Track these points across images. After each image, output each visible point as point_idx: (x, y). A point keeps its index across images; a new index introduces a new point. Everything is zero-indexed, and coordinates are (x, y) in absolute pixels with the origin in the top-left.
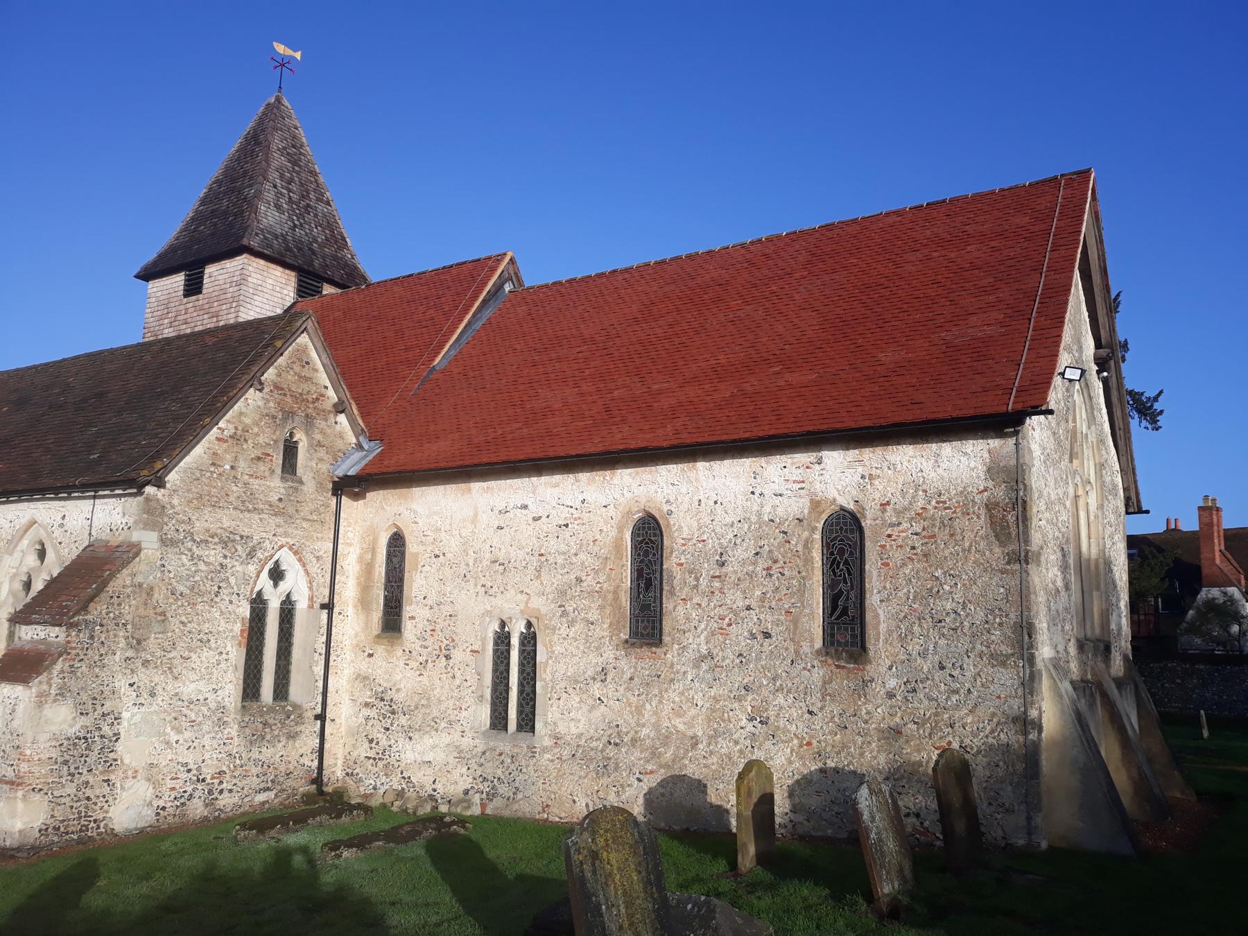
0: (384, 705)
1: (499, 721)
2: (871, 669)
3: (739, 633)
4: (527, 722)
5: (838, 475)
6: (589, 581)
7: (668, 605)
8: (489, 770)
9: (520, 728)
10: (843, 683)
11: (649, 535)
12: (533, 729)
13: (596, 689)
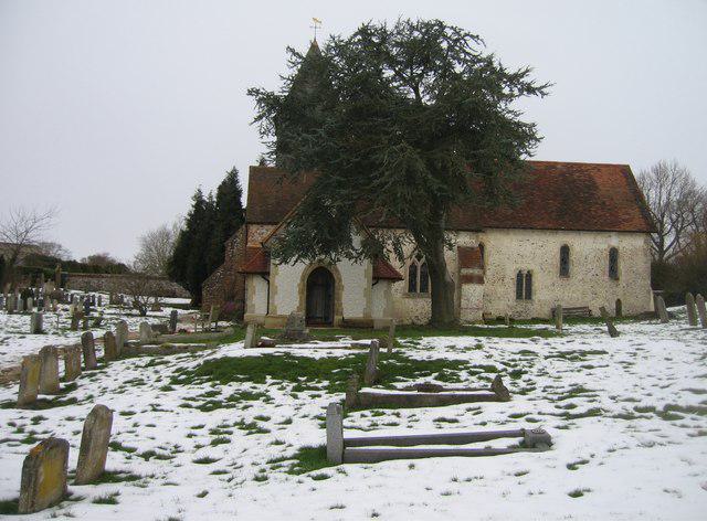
1: (519, 296)
4: (529, 296)
5: (614, 241)
6: (550, 261)
8: (518, 310)
11: (565, 250)
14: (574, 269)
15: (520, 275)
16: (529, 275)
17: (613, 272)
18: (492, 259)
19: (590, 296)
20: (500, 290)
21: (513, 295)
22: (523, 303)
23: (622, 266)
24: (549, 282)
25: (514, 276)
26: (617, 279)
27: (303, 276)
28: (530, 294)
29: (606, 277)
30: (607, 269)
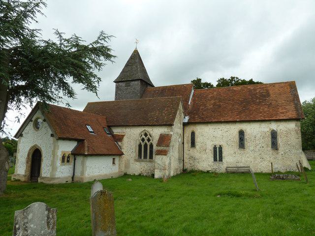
0: (191, 158)
1: (215, 160)
2: (279, 151)
3: (259, 146)
4: (221, 160)
5: (274, 126)
7: (246, 143)
9: (219, 161)
10: (274, 153)
11: (241, 133)
12: (222, 161)
13: (234, 155)
14: (247, 144)
15: (215, 148)
16: (221, 148)
17: (274, 145)
18: (198, 140)
19: (259, 160)
20: (204, 156)
21: (212, 159)
22: (217, 163)
23: (280, 141)
24: (232, 152)
25: (212, 148)
26: (277, 149)
27: (30, 150)
28: (222, 159)
29: (270, 148)
30: (270, 143)
